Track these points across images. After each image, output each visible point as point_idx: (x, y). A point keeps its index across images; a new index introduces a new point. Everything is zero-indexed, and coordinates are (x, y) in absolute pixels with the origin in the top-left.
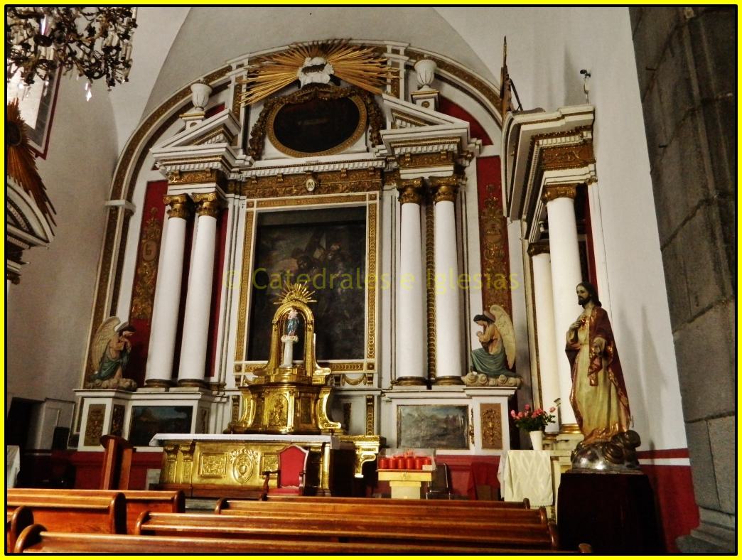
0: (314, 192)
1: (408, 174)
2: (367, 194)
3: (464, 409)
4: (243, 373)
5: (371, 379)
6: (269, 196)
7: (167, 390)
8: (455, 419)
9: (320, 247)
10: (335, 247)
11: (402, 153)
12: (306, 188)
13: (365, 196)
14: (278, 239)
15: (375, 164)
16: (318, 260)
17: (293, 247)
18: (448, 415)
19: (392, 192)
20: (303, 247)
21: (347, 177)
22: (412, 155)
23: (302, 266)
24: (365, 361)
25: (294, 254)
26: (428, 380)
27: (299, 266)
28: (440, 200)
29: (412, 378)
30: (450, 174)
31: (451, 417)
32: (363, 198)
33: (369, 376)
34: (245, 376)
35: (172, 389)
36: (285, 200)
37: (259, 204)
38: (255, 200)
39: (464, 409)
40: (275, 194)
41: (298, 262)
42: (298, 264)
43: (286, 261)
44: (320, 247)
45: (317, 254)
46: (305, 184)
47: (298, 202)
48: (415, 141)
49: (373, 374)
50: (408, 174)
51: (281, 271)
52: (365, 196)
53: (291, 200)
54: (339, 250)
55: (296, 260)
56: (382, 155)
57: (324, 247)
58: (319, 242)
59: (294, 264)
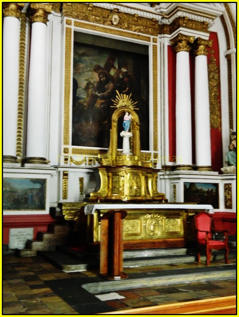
0: (116, 26)
1: (183, 31)
2: (152, 37)
3: (216, 185)
4: (70, 154)
5: (155, 164)
6: (82, 19)
7: (23, 165)
8: (212, 190)
9: (114, 68)
10: (124, 70)
11: (182, 16)
12: (111, 21)
13: (149, 38)
14: (84, 55)
15: (154, 16)
16: (113, 77)
17: (95, 63)
18: (209, 189)
19: (165, 40)
20: (102, 65)
21: (137, 21)
22: (190, 20)
23: (102, 79)
24: (152, 151)
25: (97, 69)
26: (194, 167)
27: (100, 79)
28: (201, 54)
29: (189, 166)
30: (207, 38)
31: (210, 190)
32: (148, 39)
33: (155, 162)
34: (71, 158)
35: (27, 165)
36: (95, 26)
37: (76, 24)
38: (73, 20)
39: (216, 185)
40: (86, 18)
41: (99, 75)
42: (99, 77)
43: (90, 73)
44: (114, 68)
45: (112, 72)
46: (112, 18)
47: (105, 30)
48: (193, 10)
49: (156, 161)
50: (183, 31)
51: (87, 80)
52: (149, 38)
53: (98, 27)
54: (126, 72)
55: (98, 74)
56: (161, 12)
57: (117, 67)
58: (113, 64)
59: (95, 77)
